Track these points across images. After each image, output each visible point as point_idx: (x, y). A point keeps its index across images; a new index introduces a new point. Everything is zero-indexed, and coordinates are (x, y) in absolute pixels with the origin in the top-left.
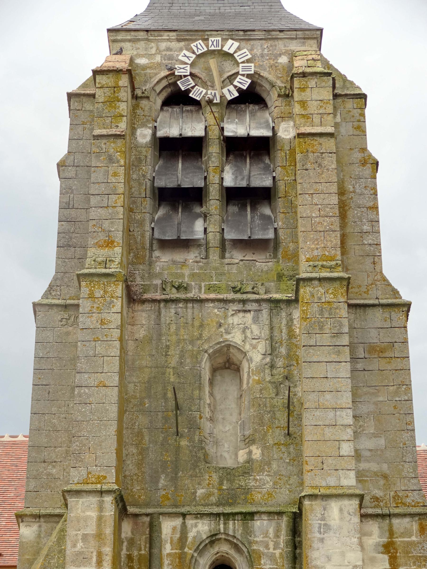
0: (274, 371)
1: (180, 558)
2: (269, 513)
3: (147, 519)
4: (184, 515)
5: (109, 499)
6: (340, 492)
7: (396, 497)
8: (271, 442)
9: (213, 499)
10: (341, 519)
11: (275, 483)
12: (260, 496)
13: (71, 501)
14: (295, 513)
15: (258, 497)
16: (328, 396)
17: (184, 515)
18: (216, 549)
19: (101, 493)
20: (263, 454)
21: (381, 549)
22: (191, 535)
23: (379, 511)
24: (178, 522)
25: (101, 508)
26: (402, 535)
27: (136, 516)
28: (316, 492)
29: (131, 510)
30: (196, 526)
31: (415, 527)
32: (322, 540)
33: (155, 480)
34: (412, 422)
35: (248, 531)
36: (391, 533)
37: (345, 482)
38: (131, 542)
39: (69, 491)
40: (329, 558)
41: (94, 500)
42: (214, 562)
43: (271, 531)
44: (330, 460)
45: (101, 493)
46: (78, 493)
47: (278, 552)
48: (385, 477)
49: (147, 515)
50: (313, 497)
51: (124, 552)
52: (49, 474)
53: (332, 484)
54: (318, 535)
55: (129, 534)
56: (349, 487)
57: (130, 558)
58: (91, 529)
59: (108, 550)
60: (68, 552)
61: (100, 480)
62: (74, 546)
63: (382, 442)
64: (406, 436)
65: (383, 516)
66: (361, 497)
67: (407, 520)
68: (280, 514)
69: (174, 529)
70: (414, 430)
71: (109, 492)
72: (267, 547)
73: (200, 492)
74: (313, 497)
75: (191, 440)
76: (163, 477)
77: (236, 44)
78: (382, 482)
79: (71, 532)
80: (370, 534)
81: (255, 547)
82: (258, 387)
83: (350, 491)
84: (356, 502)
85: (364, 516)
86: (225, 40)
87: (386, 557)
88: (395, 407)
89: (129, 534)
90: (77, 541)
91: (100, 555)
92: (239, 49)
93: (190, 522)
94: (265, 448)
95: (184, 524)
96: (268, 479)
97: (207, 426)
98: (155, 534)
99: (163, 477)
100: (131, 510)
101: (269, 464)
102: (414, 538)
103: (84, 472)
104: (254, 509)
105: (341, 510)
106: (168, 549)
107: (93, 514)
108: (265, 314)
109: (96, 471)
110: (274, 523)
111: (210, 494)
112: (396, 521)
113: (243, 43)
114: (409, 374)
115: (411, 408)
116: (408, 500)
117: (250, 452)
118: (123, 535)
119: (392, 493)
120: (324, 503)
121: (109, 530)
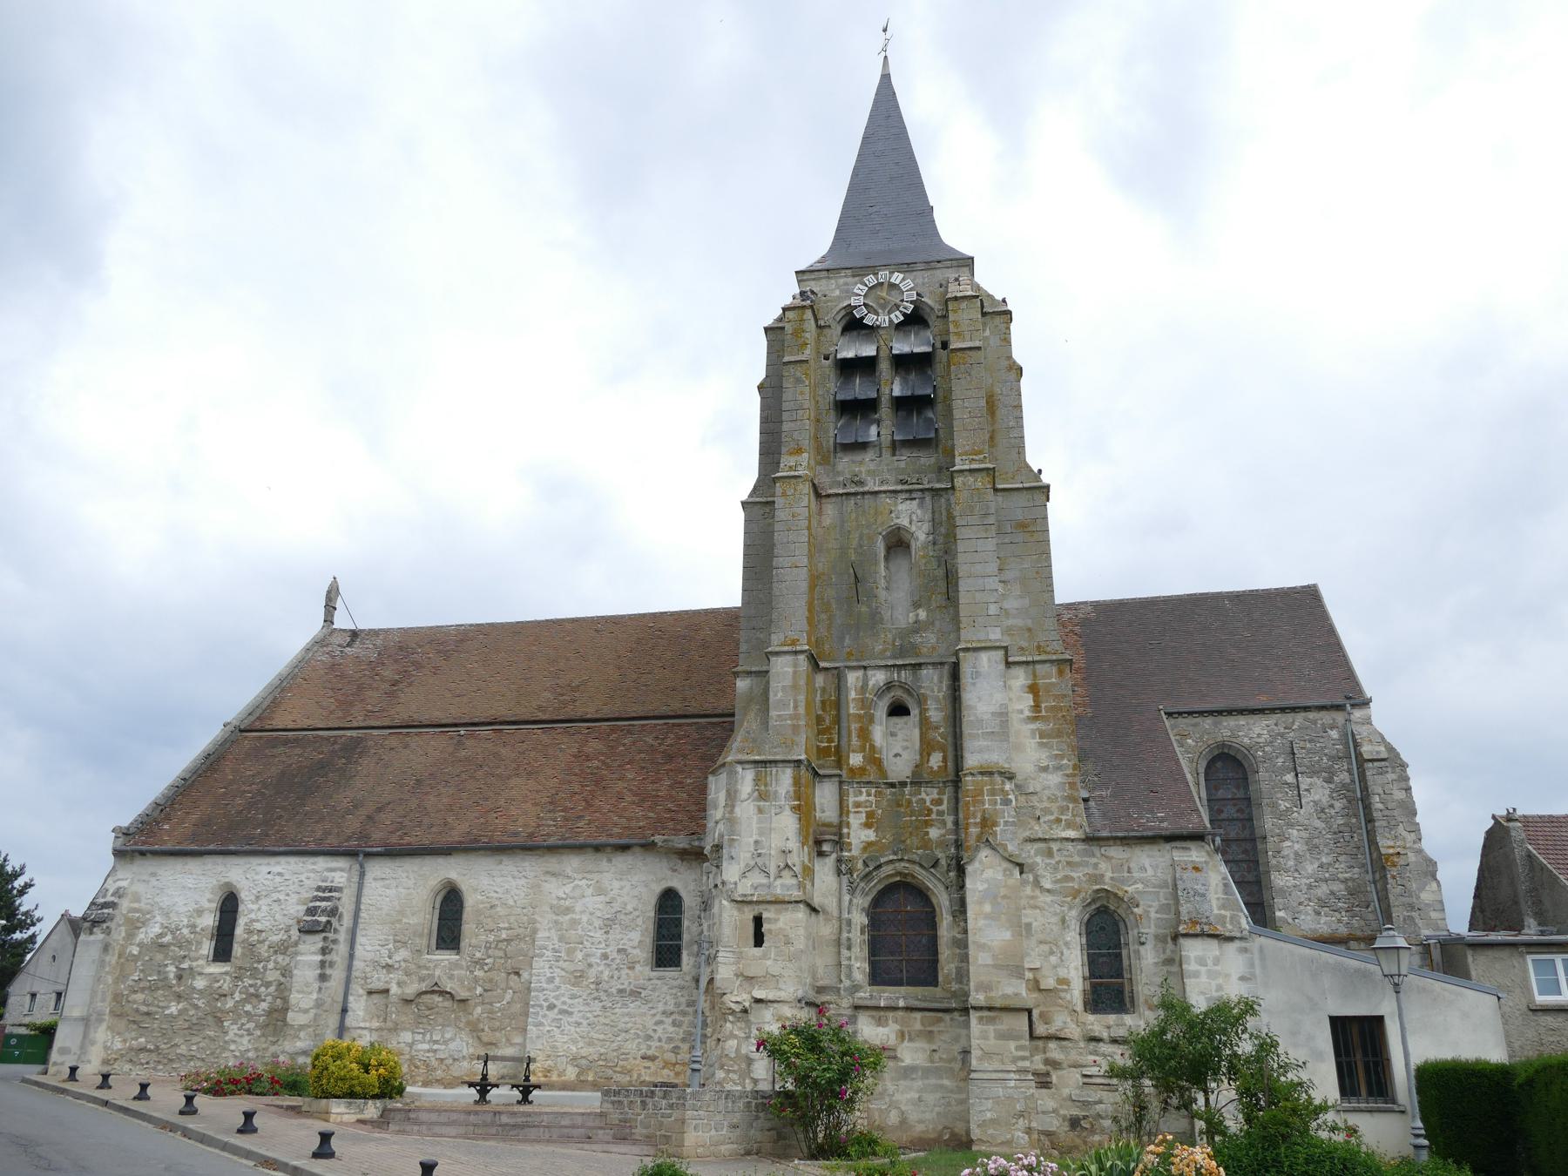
0: (936, 547)
1: (863, 701)
2: (933, 664)
3: (835, 672)
4: (865, 668)
5: (802, 657)
6: (989, 644)
7: (1039, 647)
8: (934, 605)
9: (888, 654)
10: (989, 667)
11: (938, 639)
12: (926, 650)
13: (773, 659)
14: (954, 663)
15: (925, 650)
16: (978, 567)
17: (865, 668)
18: (893, 694)
19: (796, 653)
20: (928, 616)
21: (1027, 690)
22: (871, 683)
23: (1024, 659)
24: (860, 673)
25: (795, 665)
26: (1044, 677)
27: (826, 669)
28: (969, 645)
29: (822, 664)
30: (874, 675)
31: (1054, 670)
32: (974, 684)
33: (842, 639)
34: (1051, 585)
35: (917, 679)
36: (1035, 676)
37: (992, 637)
38: (824, 690)
39: (770, 653)
40: (980, 699)
41: (789, 658)
42: (891, 704)
43: (936, 678)
44: (980, 619)
45: (796, 653)
46: (777, 654)
47: (941, 695)
48: (1029, 630)
49: (836, 668)
50: (967, 650)
51: (818, 698)
52: (757, 639)
53: (982, 638)
54: (970, 680)
55: (822, 684)
56: (996, 641)
57: (823, 702)
58: (788, 682)
59: (802, 698)
60: (771, 700)
61: (794, 643)
62: (776, 695)
63: (1027, 601)
64: (1046, 595)
65: (1027, 663)
66: (1006, 649)
67: (1048, 665)
68: (942, 664)
69: (858, 678)
70: (1053, 591)
71: (802, 652)
72: (933, 691)
73: (879, 648)
74: (967, 650)
75: (869, 606)
76: (847, 637)
77: (901, 276)
78: (1027, 635)
79: (773, 684)
80: (1017, 678)
81: (922, 691)
82: (924, 561)
83: (998, 644)
84: (1001, 653)
85: (1008, 664)
86: (892, 273)
87: (1031, 696)
88: (1037, 573)
89: (822, 684)
90: (777, 691)
91: (796, 701)
92: (903, 279)
93: (870, 673)
94: (929, 611)
95: (865, 675)
96: (932, 636)
97: (882, 594)
98: (842, 684)
99: (847, 637)
100: (822, 664)
101: (933, 623)
102: (1054, 680)
103: (782, 637)
104: (922, 661)
105: (989, 660)
106: (853, 695)
107: (790, 670)
108: (928, 499)
109: (792, 635)
110: (937, 672)
111: (885, 650)
112: (1038, 667)
113: (907, 274)
114: (1049, 545)
115: (1051, 573)
116: (1049, 649)
117: (917, 615)
118: (817, 685)
119: (1036, 644)
120: (975, 654)
121: (802, 682)
